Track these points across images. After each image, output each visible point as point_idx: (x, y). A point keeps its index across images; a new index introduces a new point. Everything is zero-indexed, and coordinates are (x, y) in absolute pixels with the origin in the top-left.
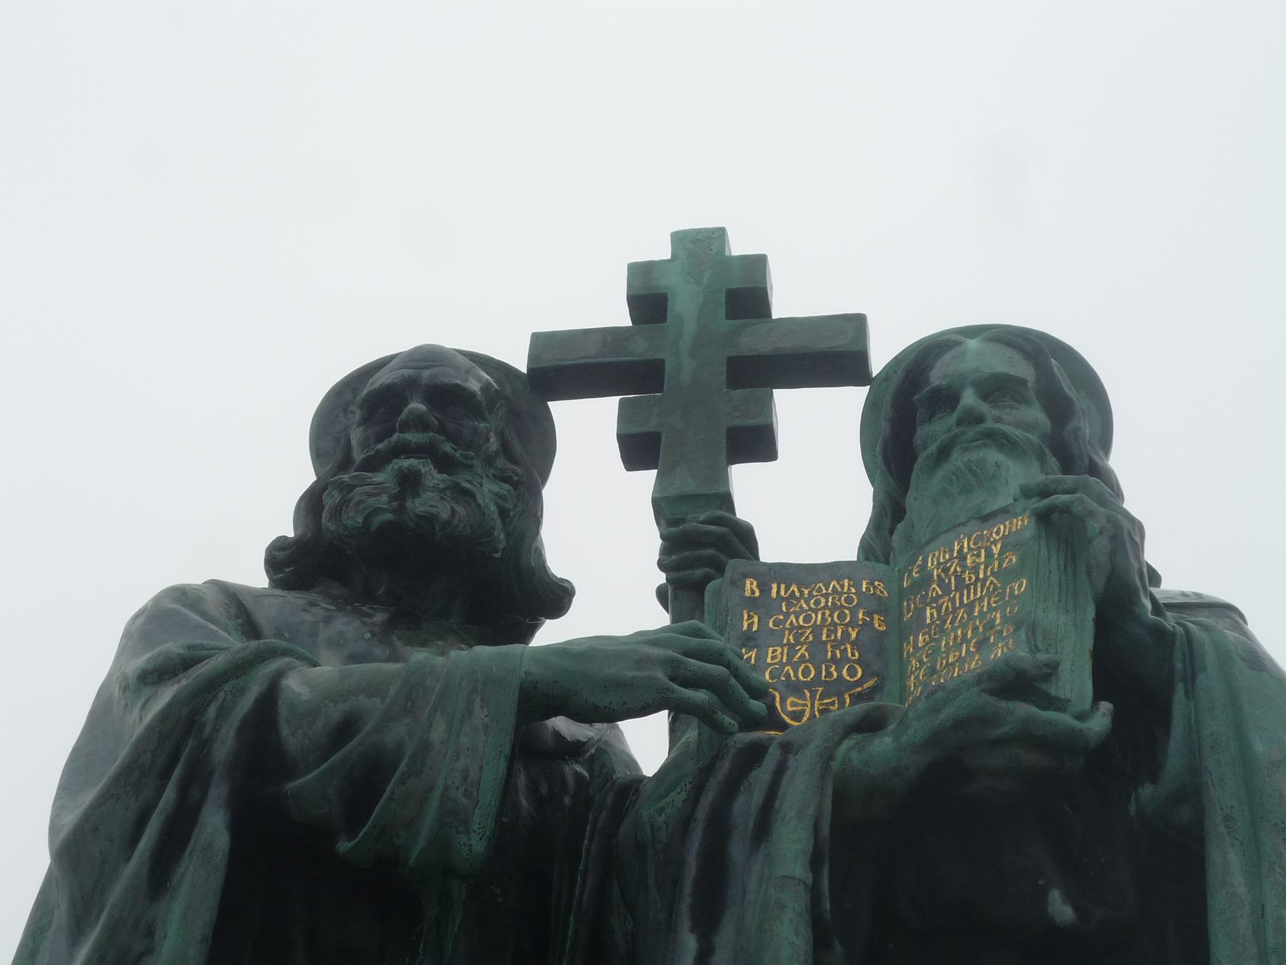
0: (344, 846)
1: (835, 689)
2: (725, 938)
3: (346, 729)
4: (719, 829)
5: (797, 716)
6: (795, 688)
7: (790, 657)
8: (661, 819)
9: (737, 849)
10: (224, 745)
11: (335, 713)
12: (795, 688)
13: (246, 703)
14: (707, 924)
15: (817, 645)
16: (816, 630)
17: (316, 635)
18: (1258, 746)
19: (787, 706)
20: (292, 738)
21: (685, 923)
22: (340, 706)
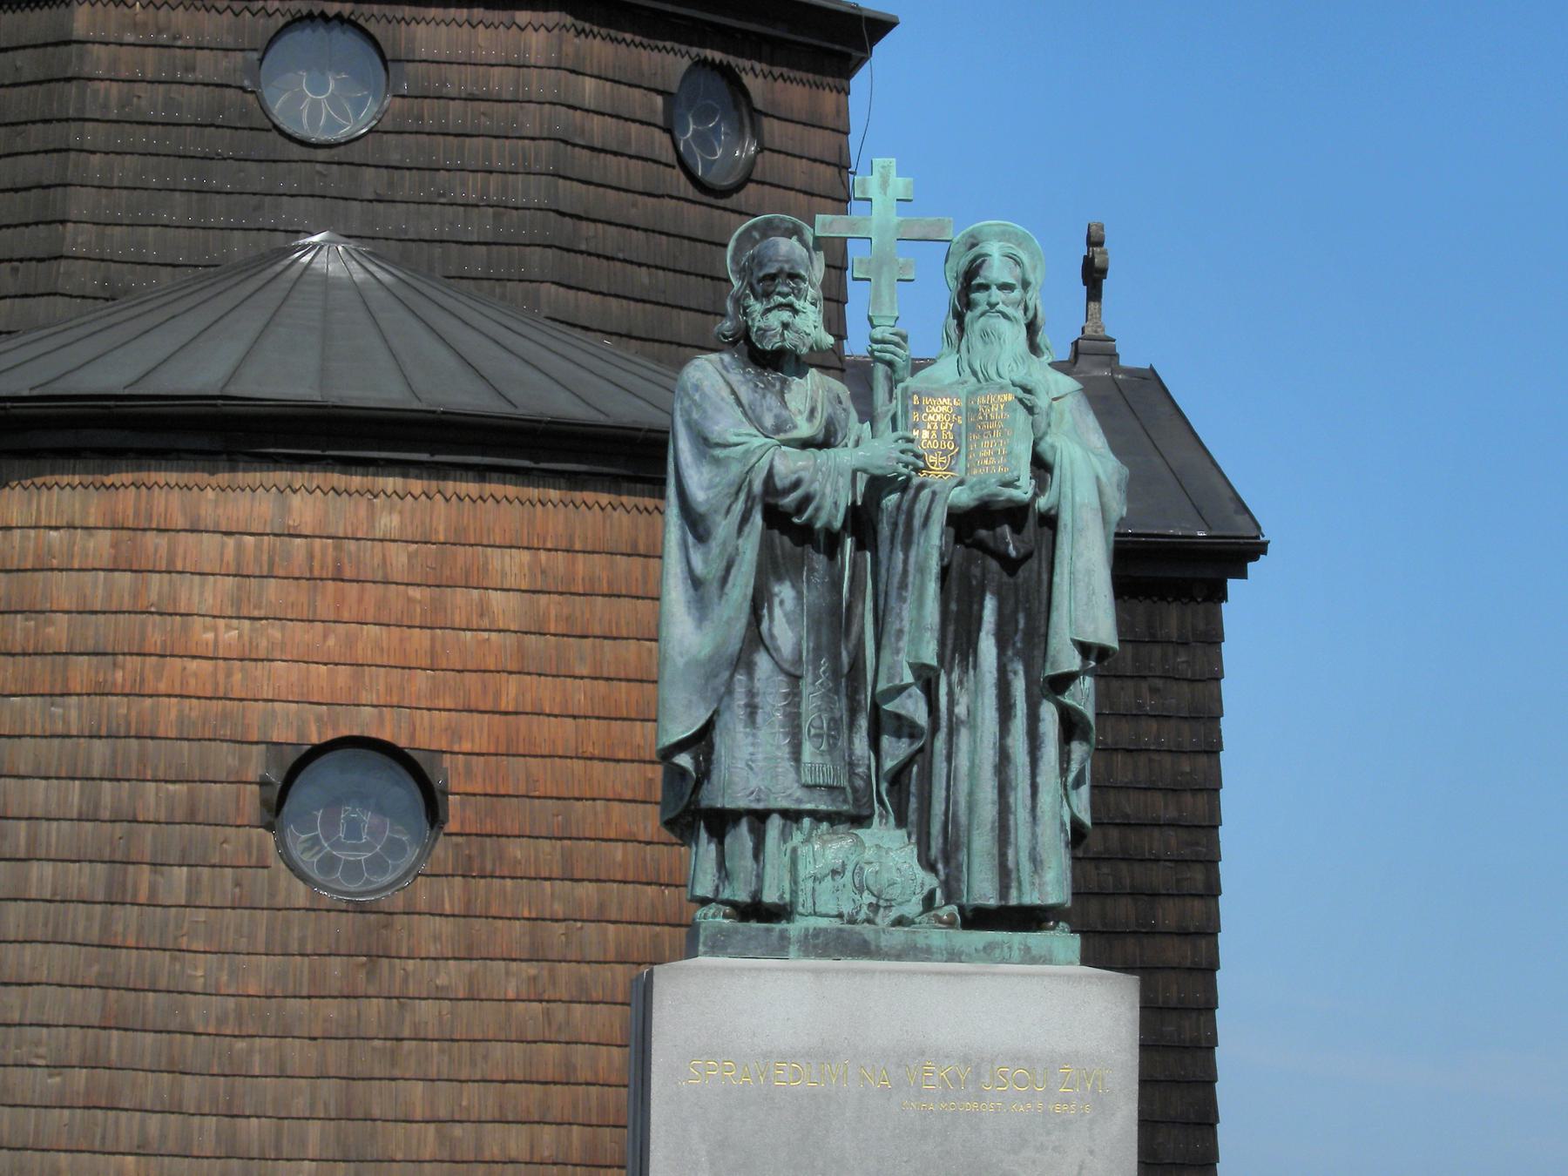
0: (796, 520)
1: (945, 452)
2: (913, 554)
3: (796, 484)
4: (910, 515)
5: (933, 464)
6: (932, 452)
7: (930, 436)
8: (889, 504)
9: (917, 522)
10: (758, 486)
11: (794, 477)
12: (932, 452)
13: (764, 474)
14: (907, 544)
15: (939, 432)
16: (939, 423)
17: (762, 406)
18: (1078, 499)
19: (931, 459)
20: (780, 483)
21: (899, 547)
22: (796, 476)
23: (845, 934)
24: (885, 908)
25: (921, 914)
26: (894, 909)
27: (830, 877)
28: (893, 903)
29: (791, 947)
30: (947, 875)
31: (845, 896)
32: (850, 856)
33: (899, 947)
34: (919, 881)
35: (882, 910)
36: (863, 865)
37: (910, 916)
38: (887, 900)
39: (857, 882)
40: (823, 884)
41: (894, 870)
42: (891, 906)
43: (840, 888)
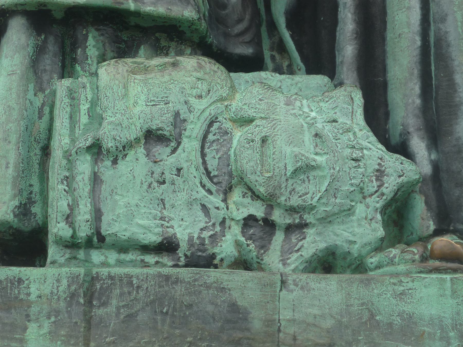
23: (179, 290)
24: (289, 229)
25: (378, 249)
26: (310, 232)
27: (141, 151)
28: (309, 218)
29: (32, 328)
30: (436, 167)
31: (182, 197)
32: (192, 100)
33: (329, 323)
34: (373, 165)
35: (279, 237)
36: (228, 125)
37: (355, 250)
38: (292, 210)
39: (212, 164)
40: (122, 166)
41: (308, 137)
42: (303, 226)
43: (168, 176)
